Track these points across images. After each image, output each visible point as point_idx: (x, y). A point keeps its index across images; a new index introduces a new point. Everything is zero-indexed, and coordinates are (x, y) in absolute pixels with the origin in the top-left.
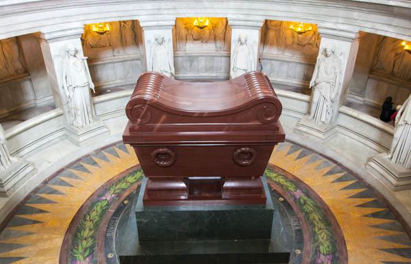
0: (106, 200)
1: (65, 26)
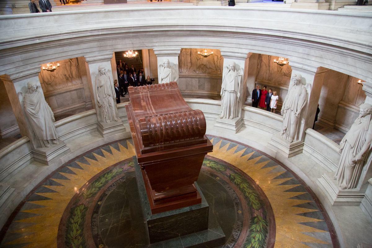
1: (236, 50)
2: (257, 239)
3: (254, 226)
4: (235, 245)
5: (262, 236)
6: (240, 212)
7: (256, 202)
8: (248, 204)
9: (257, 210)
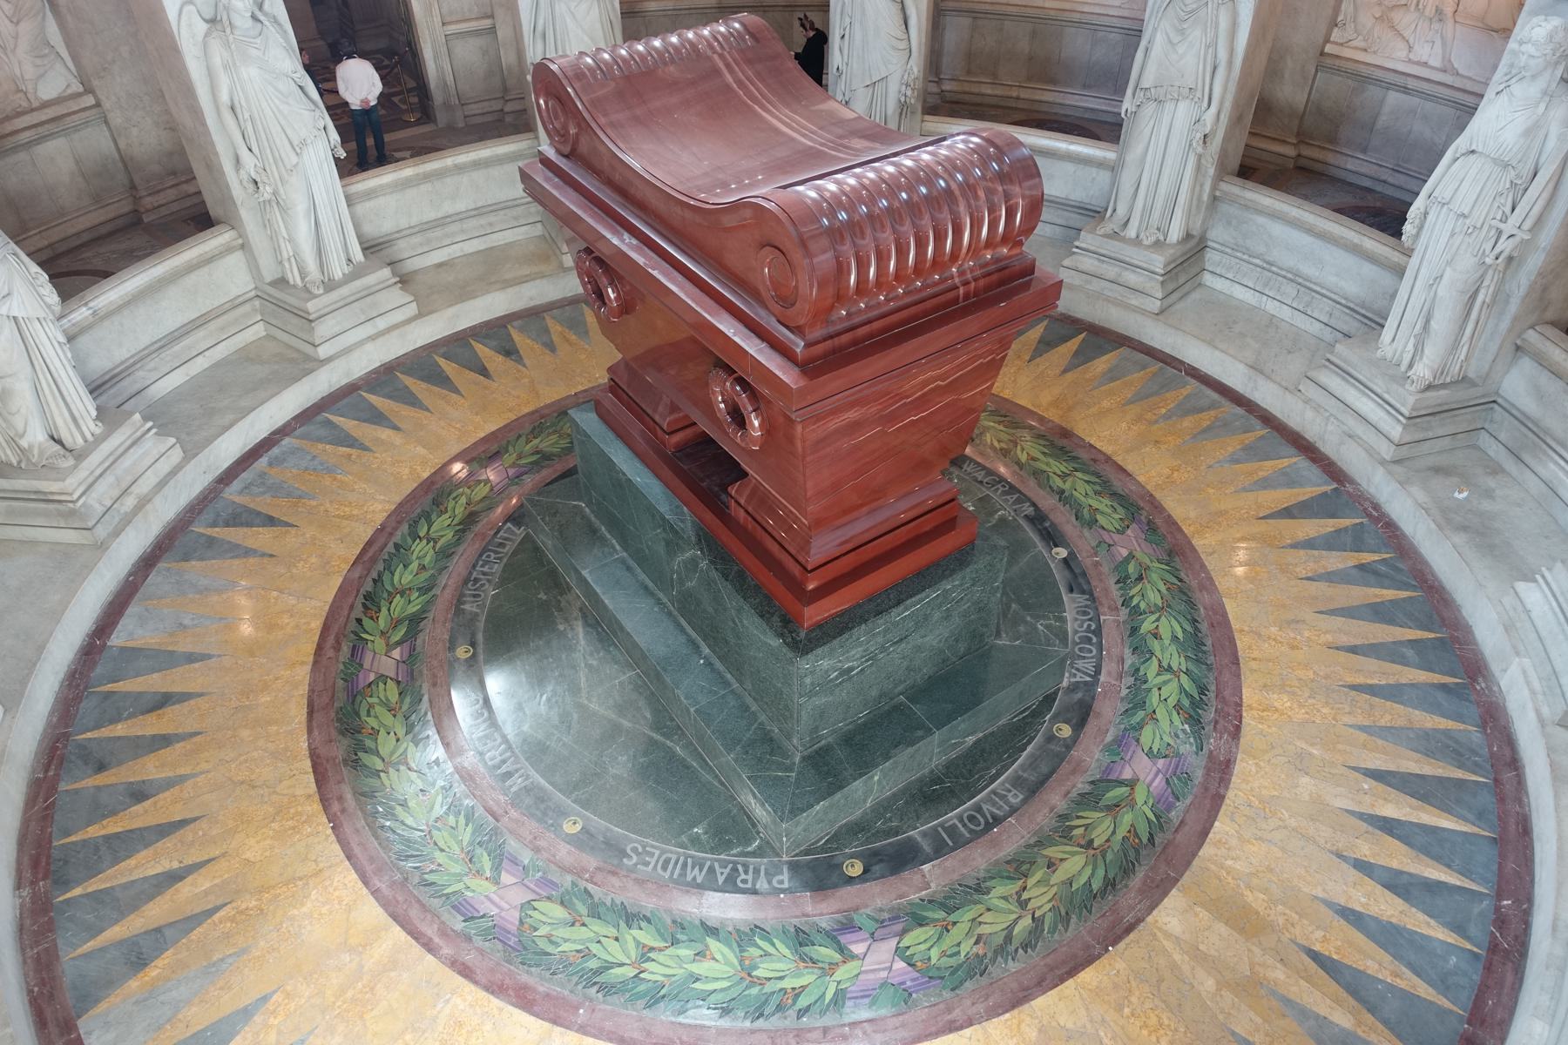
2: (414, 566)
9: (383, 678)
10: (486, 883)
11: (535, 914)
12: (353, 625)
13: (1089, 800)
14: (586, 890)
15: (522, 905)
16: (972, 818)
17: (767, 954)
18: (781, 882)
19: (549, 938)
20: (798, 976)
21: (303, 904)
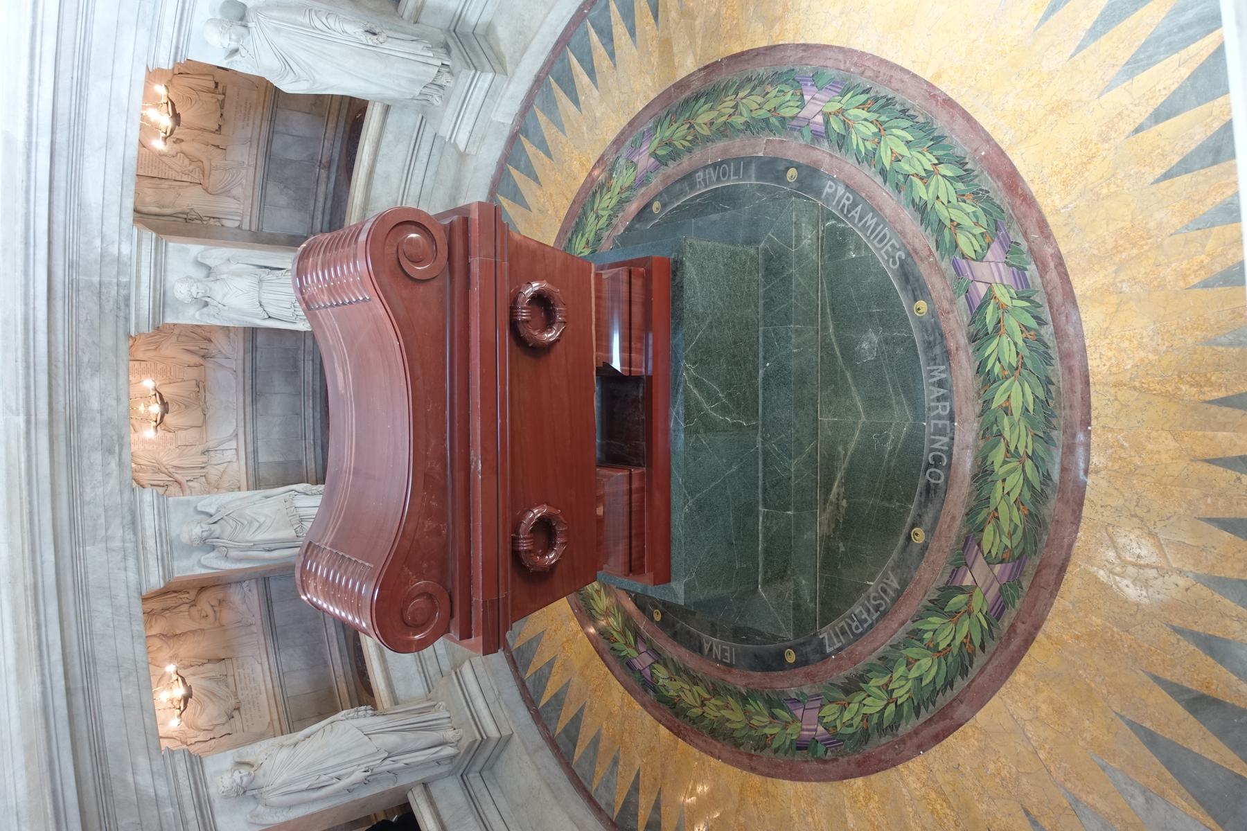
0: (802, 107)
2: (914, 673)
3: (935, 621)
4: (843, 652)
5: (937, 673)
6: (920, 536)
7: (1011, 520)
8: (971, 513)
10: (998, 294)
11: (978, 248)
12: (991, 646)
13: (675, 155)
14: (937, 248)
15: (981, 261)
16: (724, 175)
17: (864, 140)
18: (831, 187)
19: (977, 224)
20: (857, 116)
21: (1142, 360)
